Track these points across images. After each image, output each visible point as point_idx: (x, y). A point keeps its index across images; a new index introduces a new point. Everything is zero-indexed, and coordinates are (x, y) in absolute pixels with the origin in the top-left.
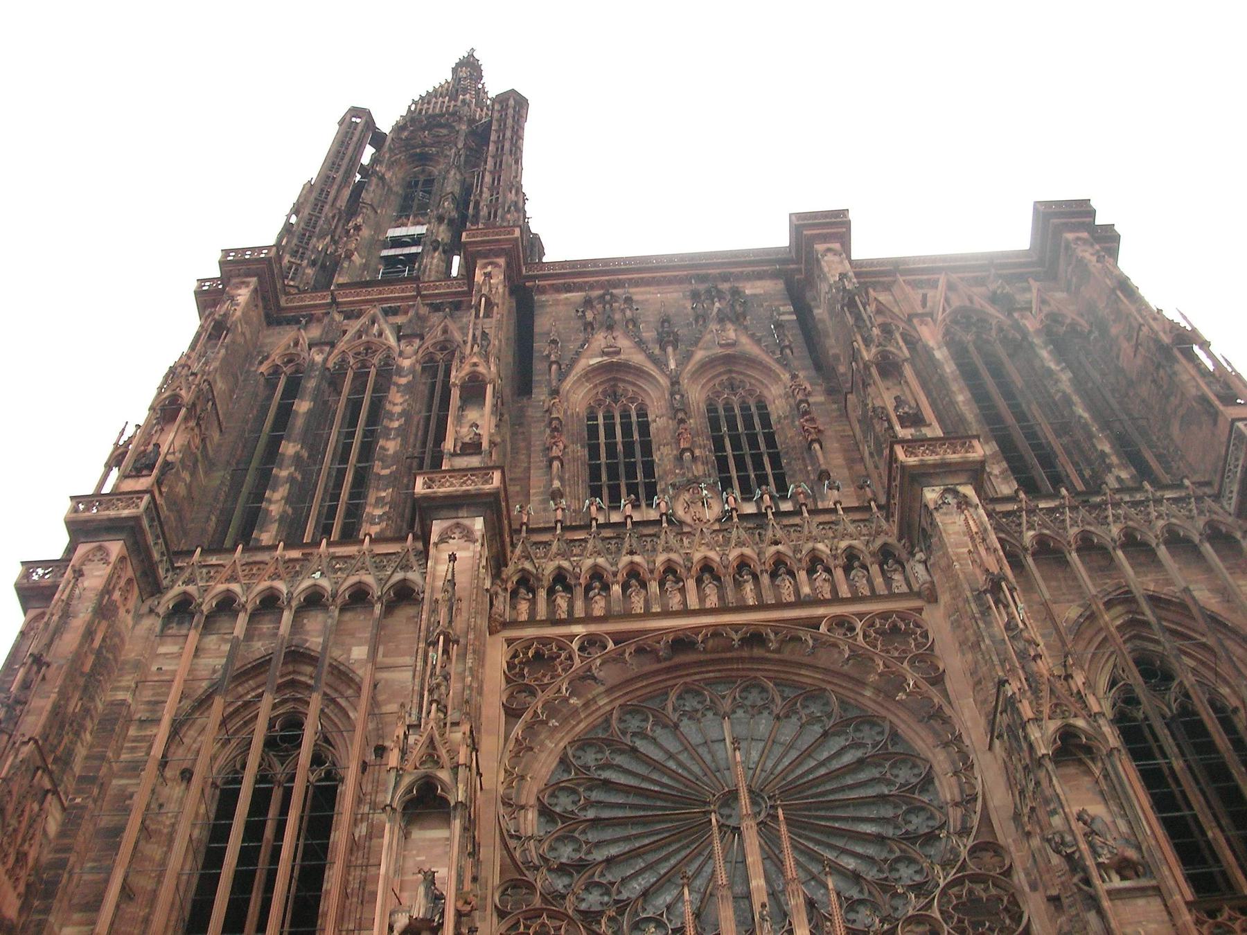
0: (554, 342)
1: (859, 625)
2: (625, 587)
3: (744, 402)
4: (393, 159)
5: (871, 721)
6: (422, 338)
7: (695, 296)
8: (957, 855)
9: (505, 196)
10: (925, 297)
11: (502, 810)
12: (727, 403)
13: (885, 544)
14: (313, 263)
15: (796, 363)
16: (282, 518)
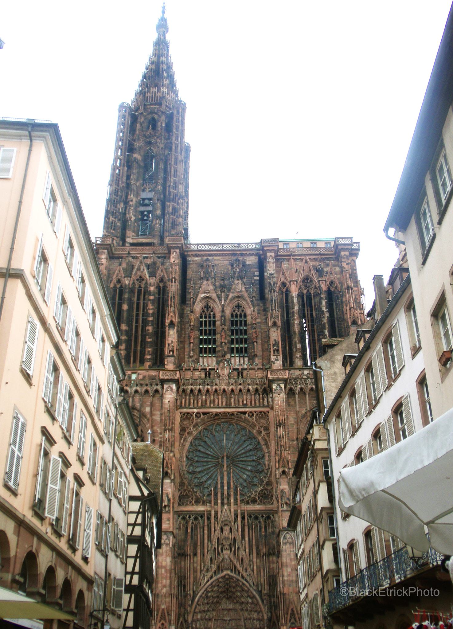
0: (192, 287)
1: (255, 414)
2: (206, 395)
3: (241, 314)
4: (140, 145)
5: (255, 438)
6: (156, 277)
7: (232, 265)
8: (264, 482)
9: (178, 187)
10: (297, 270)
11: (179, 462)
12: (236, 314)
13: (265, 387)
14: (119, 220)
15: (256, 302)
16: (125, 359)
